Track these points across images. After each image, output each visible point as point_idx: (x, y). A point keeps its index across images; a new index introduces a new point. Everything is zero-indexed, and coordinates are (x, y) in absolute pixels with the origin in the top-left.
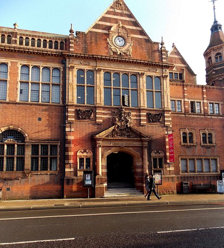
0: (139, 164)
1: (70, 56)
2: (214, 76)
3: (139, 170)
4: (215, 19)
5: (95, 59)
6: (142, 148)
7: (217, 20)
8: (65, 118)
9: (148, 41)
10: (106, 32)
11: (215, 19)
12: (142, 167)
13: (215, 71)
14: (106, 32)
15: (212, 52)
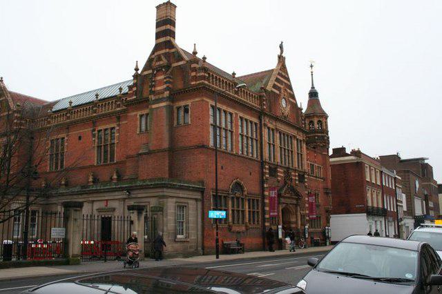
0: (293, 220)
1: (265, 114)
2: (317, 141)
3: (293, 226)
4: (313, 84)
5: (277, 119)
6: (296, 205)
7: (315, 86)
8: (263, 174)
9: (296, 104)
10: (277, 92)
11: (313, 84)
12: (296, 223)
13: (317, 136)
14: (277, 92)
15: (315, 118)
